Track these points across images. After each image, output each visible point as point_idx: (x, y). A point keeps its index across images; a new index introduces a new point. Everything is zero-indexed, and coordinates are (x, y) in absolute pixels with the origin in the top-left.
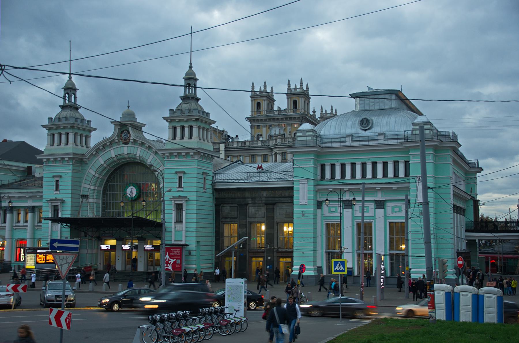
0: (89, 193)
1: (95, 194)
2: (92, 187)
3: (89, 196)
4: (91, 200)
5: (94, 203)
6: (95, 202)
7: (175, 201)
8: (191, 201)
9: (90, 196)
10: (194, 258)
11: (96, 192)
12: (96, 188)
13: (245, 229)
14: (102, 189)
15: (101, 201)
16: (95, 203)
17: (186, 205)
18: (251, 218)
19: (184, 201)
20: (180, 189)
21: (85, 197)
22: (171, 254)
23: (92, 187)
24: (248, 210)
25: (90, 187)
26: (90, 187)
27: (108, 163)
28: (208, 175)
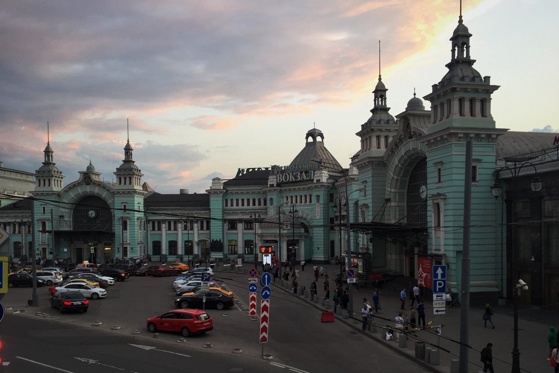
0: (392, 196)
1: (397, 197)
2: (393, 190)
3: (391, 200)
4: (393, 204)
5: (396, 206)
6: (397, 205)
7: (433, 200)
8: (449, 199)
9: (392, 200)
10: (453, 273)
11: (397, 194)
12: (397, 190)
13: (539, 234)
14: (406, 191)
15: (405, 204)
16: (398, 206)
17: (445, 205)
18: (547, 217)
19: (440, 200)
20: (439, 185)
21: (388, 200)
22: (424, 266)
23: (393, 190)
24: (543, 206)
25: (391, 190)
26: (391, 190)
27: (402, 162)
28: (482, 161)
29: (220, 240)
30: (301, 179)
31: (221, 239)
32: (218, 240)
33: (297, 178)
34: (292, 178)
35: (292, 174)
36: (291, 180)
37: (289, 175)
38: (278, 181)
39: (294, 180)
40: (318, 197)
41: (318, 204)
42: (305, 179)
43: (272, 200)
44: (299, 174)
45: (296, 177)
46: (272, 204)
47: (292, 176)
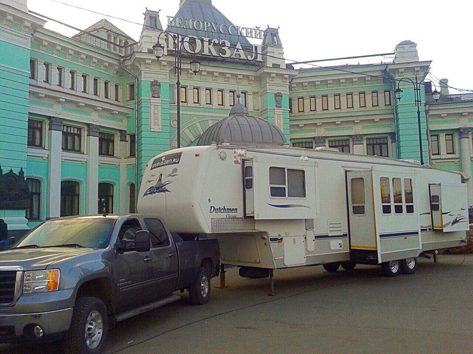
29: (21, 172)
30: (233, 56)
31: (23, 169)
32: (16, 171)
33: (224, 52)
34: (209, 49)
35: (210, 42)
36: (206, 52)
37: (202, 41)
38: (171, 48)
39: (215, 53)
40: (278, 96)
41: (277, 111)
42: (243, 57)
43: (159, 85)
44: (228, 44)
45: (220, 46)
46: (155, 95)
47: (209, 44)
